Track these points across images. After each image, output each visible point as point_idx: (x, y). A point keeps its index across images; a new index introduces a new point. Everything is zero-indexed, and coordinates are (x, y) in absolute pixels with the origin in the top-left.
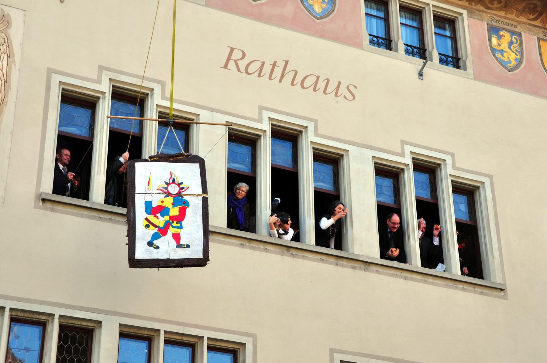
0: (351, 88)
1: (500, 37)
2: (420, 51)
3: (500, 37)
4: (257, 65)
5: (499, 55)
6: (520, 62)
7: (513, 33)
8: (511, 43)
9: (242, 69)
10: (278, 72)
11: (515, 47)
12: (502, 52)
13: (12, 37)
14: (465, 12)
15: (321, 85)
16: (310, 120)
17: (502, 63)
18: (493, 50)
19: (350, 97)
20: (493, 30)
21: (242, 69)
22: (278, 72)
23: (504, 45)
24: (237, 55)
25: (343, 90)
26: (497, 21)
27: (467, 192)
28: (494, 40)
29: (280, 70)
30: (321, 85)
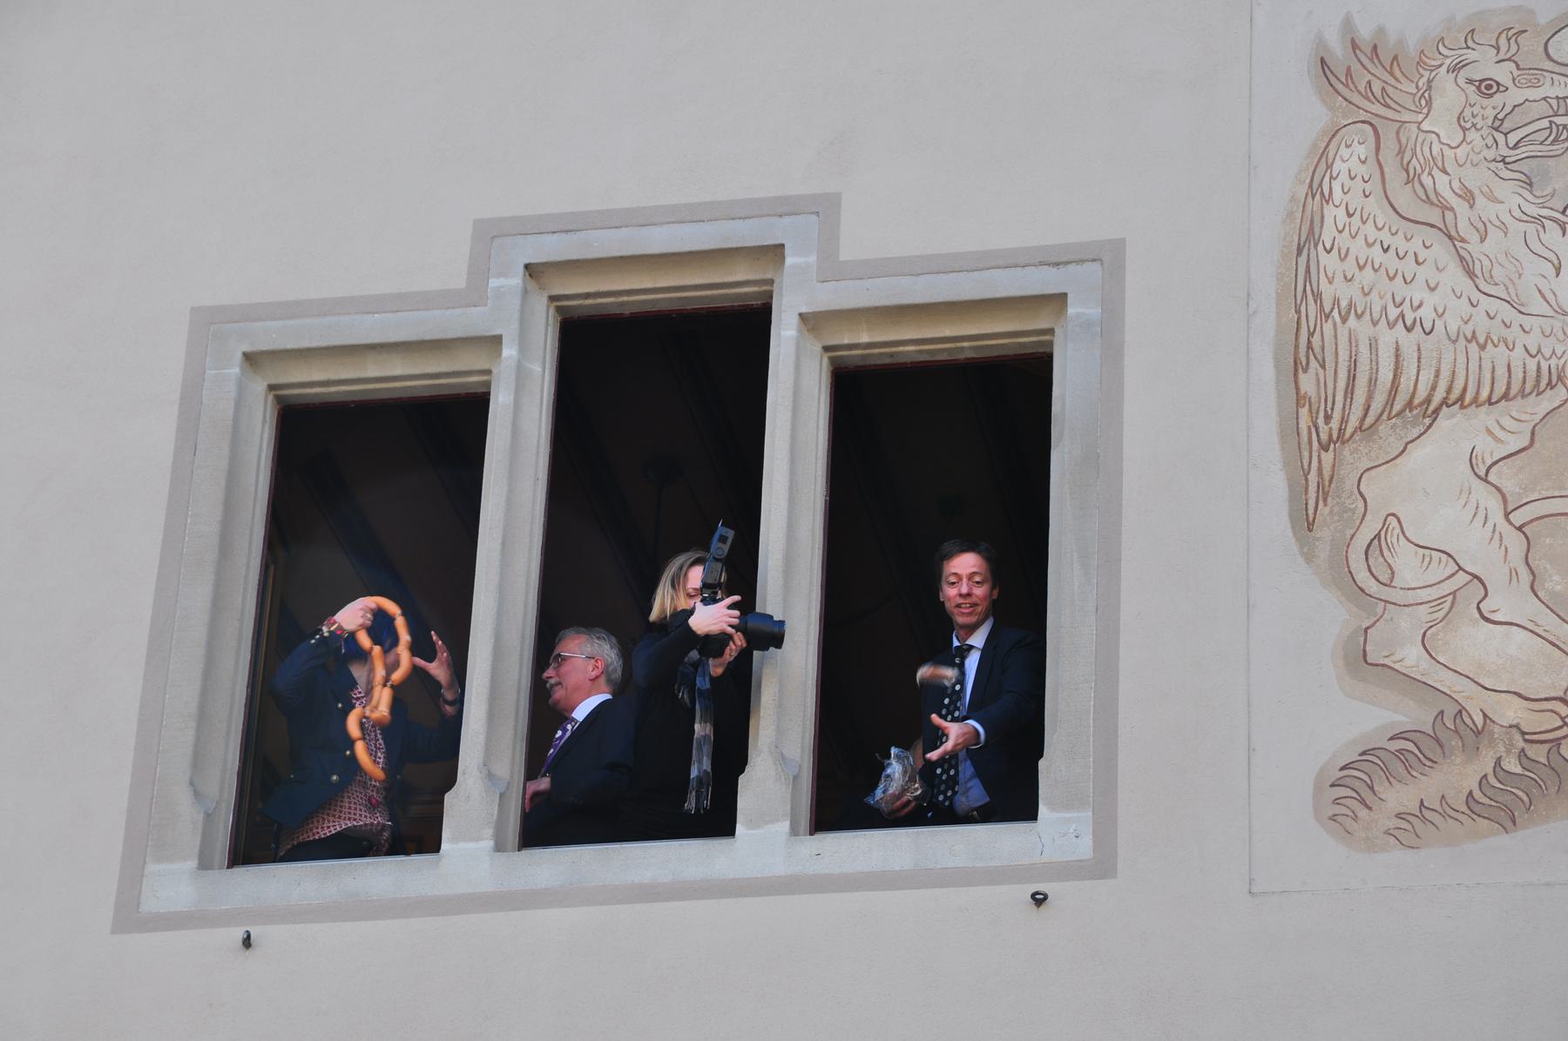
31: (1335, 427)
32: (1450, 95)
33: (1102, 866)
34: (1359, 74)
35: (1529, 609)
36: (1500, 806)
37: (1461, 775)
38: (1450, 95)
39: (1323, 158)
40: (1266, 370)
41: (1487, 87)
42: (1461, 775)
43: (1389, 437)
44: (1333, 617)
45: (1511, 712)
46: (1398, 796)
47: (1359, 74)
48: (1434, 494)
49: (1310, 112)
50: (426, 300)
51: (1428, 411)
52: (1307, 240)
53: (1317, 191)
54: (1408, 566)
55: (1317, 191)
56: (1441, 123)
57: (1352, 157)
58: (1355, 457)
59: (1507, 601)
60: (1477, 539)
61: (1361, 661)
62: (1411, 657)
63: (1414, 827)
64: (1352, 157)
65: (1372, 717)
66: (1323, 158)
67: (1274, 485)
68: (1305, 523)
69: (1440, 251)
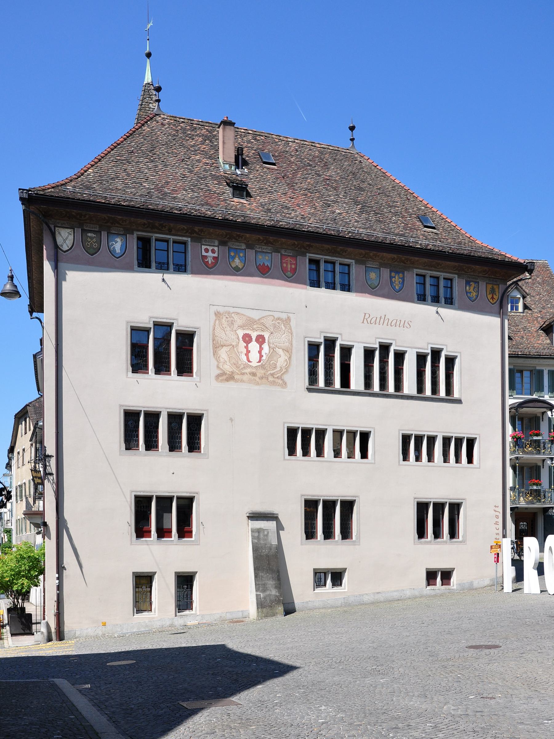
0: (409, 322)
1: (470, 285)
2: (436, 300)
3: (470, 285)
4: (374, 319)
5: (469, 295)
6: (477, 296)
7: (475, 282)
8: (475, 287)
9: (369, 322)
10: (382, 320)
11: (476, 289)
12: (470, 292)
13: (292, 325)
14: (456, 276)
15: (398, 323)
16: (394, 340)
17: (469, 298)
18: (467, 293)
19: (408, 326)
20: (468, 283)
21: (369, 322)
22: (382, 320)
23: (472, 288)
24: (367, 316)
25: (406, 324)
26: (469, 278)
27: (450, 361)
28: (468, 288)
29: (383, 320)
30: (398, 323)
31: (216, 346)
32: (224, 318)
33: (200, 382)
34: (218, 314)
35: (229, 364)
36: (227, 380)
37: (224, 377)
38: (224, 318)
39: (215, 322)
40: (211, 341)
41: (227, 318)
42: (224, 377)
43: (220, 348)
44: (216, 363)
45: (228, 373)
46: (220, 378)
47: (218, 314)
48: (223, 353)
49: (214, 318)
50: (145, 323)
51: (222, 346)
52: (214, 329)
53: (215, 325)
54: (221, 359)
55: (215, 325)
56: (224, 320)
57: (217, 322)
58: (218, 349)
59: (228, 363)
60: (226, 359)
61: (218, 367)
62: (221, 367)
63: (222, 381)
64: (217, 322)
65: (219, 372)
66: (215, 322)
67: (212, 351)
68: (214, 355)
69: (223, 332)
